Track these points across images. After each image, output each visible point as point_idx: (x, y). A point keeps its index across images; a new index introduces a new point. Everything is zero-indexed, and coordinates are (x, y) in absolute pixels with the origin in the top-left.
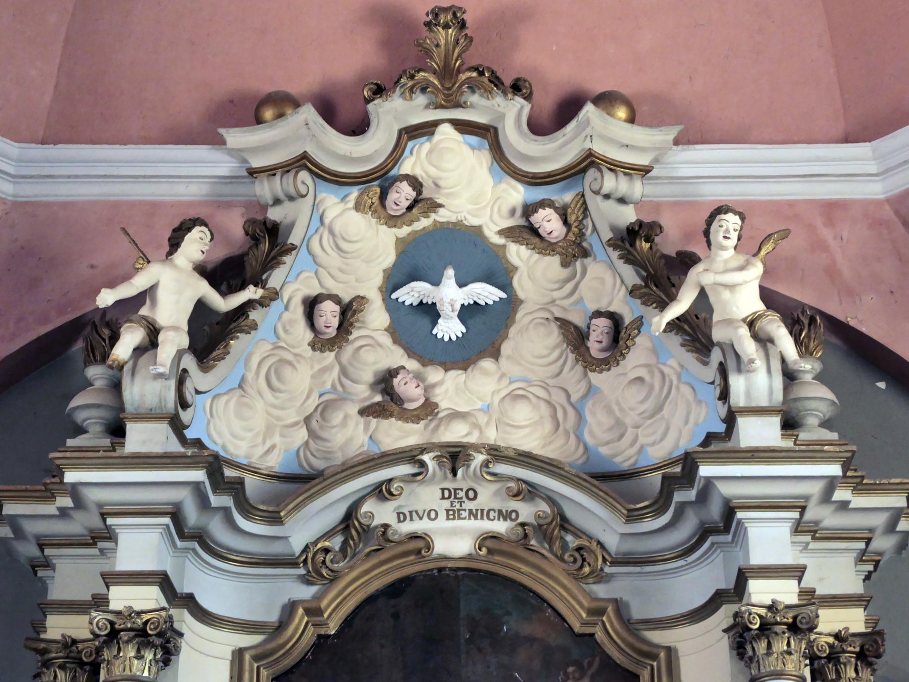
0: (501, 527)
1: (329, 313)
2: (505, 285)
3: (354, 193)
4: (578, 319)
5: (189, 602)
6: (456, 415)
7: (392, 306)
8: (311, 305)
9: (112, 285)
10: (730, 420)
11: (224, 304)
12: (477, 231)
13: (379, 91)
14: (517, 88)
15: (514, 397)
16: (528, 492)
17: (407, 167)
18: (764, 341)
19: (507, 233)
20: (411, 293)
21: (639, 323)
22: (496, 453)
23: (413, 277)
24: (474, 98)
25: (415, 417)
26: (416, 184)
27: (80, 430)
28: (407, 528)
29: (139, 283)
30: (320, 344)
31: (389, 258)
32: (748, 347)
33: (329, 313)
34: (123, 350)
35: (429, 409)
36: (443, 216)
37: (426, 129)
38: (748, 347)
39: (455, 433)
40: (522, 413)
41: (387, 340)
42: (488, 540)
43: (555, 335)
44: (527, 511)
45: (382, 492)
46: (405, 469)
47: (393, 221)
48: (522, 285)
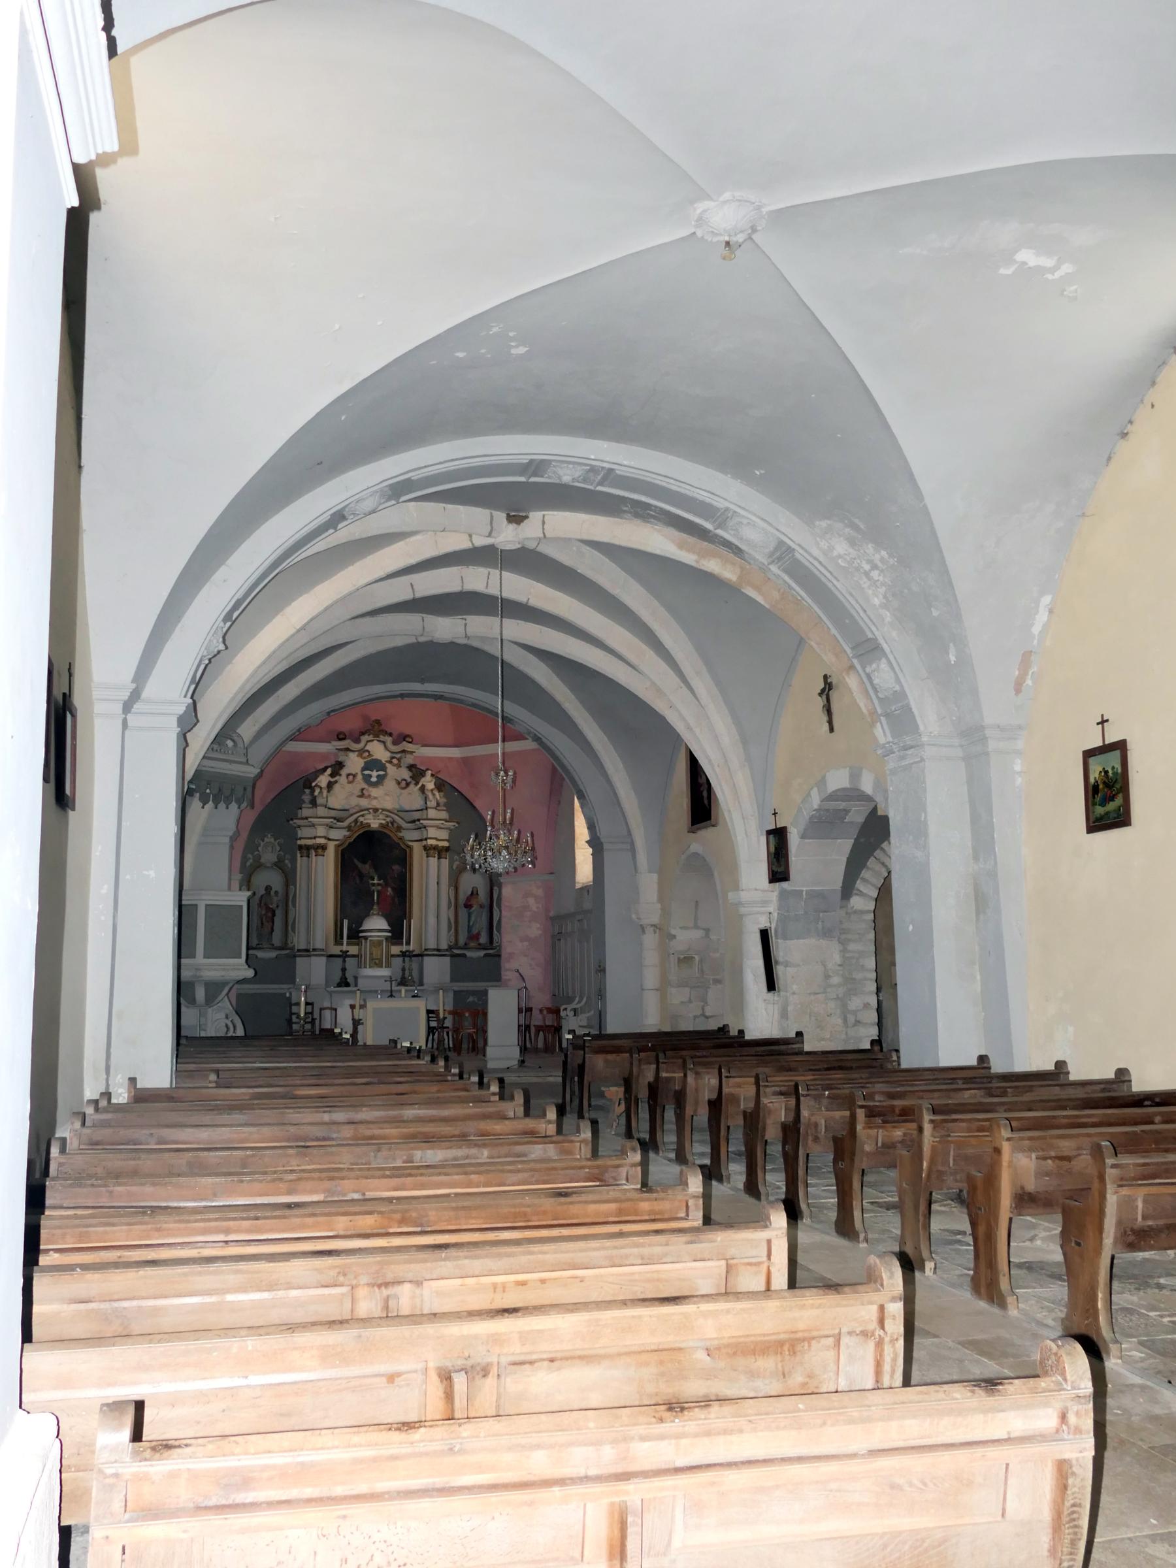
0: (384, 822)
1: (351, 777)
2: (385, 771)
3: (357, 753)
4: (399, 779)
5: (329, 839)
6: (375, 798)
7: (363, 775)
8: (348, 775)
9: (314, 781)
10: (427, 809)
11: (332, 780)
12: (380, 761)
13: (363, 734)
14: (390, 735)
15: (386, 794)
16: (387, 816)
17: (367, 748)
18: (434, 795)
19: (386, 761)
20: (366, 772)
21: (410, 782)
22: (383, 810)
23: (368, 770)
24: (381, 736)
25: (366, 798)
26: (368, 751)
27: (304, 802)
28: (365, 821)
29: (319, 779)
30: (350, 782)
31: (363, 765)
32: (430, 794)
33: (351, 777)
34: (316, 793)
35: (369, 796)
36: (374, 757)
37: (373, 741)
38: (430, 794)
39: (375, 804)
40: (388, 798)
41: (361, 781)
42: (381, 825)
43: (394, 782)
44: (388, 819)
45: (363, 816)
46: (367, 812)
47: (364, 758)
48: (388, 771)
